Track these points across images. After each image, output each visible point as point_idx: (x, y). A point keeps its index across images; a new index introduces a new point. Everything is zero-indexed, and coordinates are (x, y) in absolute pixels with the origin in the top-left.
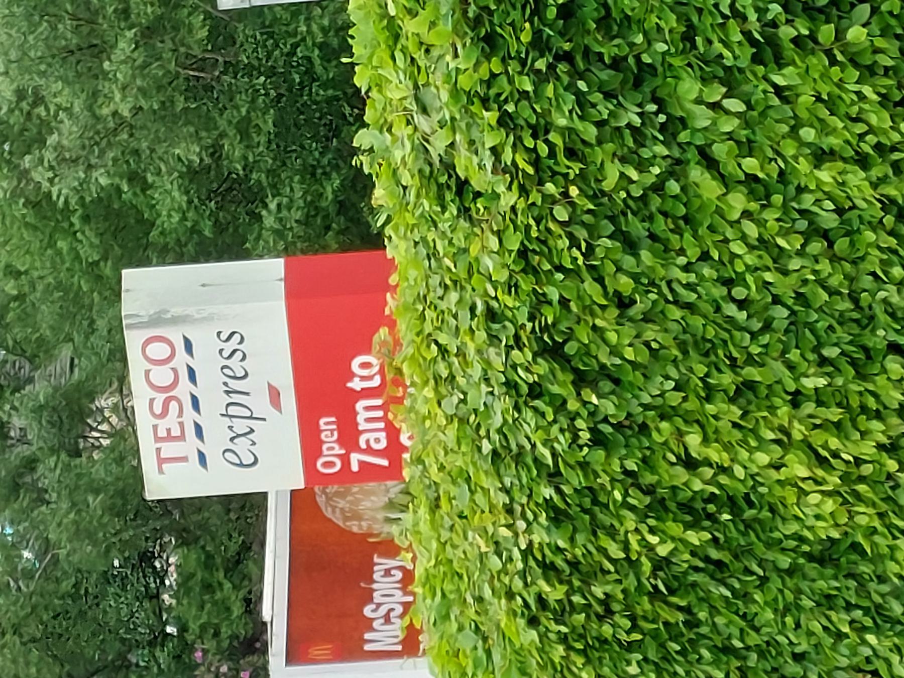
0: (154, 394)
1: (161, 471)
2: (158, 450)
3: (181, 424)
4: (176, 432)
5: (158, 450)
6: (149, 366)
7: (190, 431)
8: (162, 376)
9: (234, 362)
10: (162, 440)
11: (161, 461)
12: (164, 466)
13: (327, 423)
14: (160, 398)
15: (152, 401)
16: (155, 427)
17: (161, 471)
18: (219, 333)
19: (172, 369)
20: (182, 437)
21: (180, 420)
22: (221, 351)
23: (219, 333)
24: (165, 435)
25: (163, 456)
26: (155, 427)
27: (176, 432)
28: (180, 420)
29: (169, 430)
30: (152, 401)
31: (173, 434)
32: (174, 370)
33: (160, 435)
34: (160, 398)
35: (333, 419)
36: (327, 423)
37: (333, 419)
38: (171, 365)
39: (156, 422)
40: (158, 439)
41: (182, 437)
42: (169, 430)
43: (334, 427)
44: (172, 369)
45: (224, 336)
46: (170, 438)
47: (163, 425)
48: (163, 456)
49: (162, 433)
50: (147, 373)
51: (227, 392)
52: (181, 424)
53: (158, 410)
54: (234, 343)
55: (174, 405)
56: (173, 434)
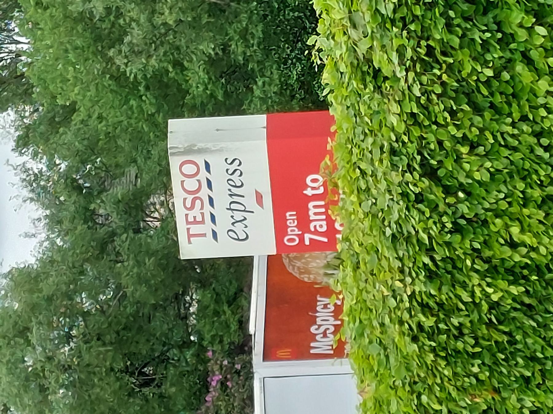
0: (186, 195)
1: (190, 242)
2: (188, 229)
3: (203, 214)
4: (199, 219)
5: (188, 229)
6: (184, 178)
7: (208, 218)
8: (191, 184)
9: (235, 177)
10: (191, 223)
11: (190, 236)
12: (191, 239)
13: (291, 215)
14: (190, 198)
15: (185, 199)
16: (187, 215)
17: (190, 242)
18: (226, 159)
19: (198, 180)
20: (203, 222)
21: (201, 211)
22: (227, 170)
23: (226, 159)
24: (193, 220)
25: (191, 233)
26: (187, 215)
27: (199, 219)
28: (201, 211)
29: (195, 217)
30: (185, 199)
31: (197, 220)
32: (199, 181)
33: (190, 220)
34: (190, 198)
35: (295, 213)
36: (291, 215)
37: (295, 213)
38: (197, 178)
39: (187, 212)
40: (188, 223)
41: (203, 222)
42: (195, 217)
43: (295, 217)
44: (198, 180)
45: (229, 161)
46: (195, 222)
48: (191, 233)
49: (191, 219)
50: (182, 182)
51: (231, 195)
52: (203, 214)
53: (188, 205)
54: (235, 165)
55: (198, 202)
56: (197, 220)
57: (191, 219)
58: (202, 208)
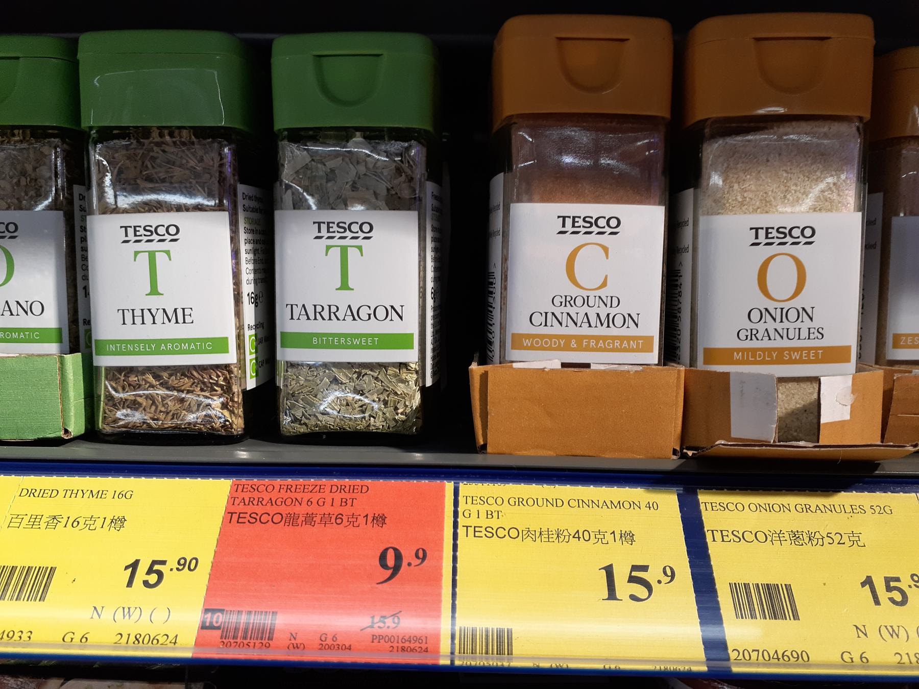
2: (569, 217)
3: (580, 227)
5: (569, 217)
12: (562, 219)
14: (593, 221)
15: (592, 218)
25: (567, 219)
26: (580, 217)
29: (578, 222)
30: (592, 218)
31: (576, 223)
39: (582, 218)
41: (573, 226)
42: (578, 222)
46: (574, 222)
47: (581, 221)
48: (567, 219)
49: (577, 219)
55: (588, 225)
56: (576, 223)
57: (577, 219)
58: (583, 227)
